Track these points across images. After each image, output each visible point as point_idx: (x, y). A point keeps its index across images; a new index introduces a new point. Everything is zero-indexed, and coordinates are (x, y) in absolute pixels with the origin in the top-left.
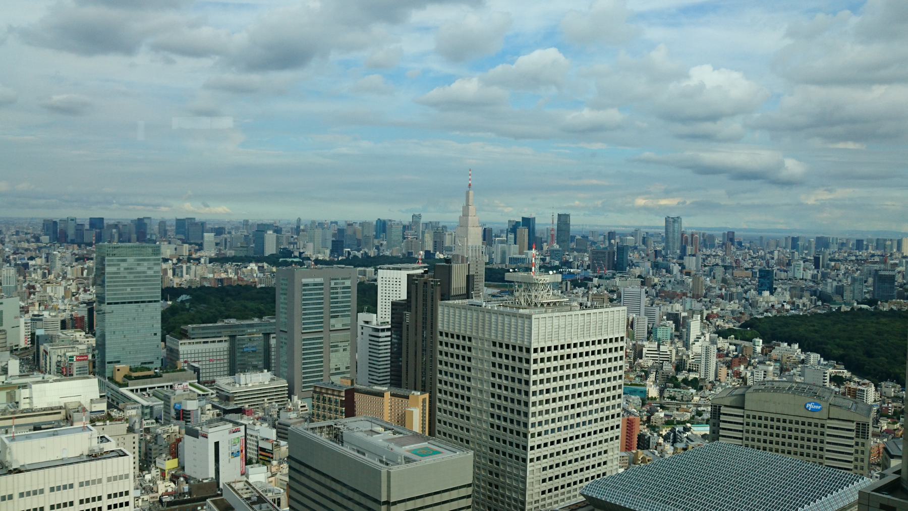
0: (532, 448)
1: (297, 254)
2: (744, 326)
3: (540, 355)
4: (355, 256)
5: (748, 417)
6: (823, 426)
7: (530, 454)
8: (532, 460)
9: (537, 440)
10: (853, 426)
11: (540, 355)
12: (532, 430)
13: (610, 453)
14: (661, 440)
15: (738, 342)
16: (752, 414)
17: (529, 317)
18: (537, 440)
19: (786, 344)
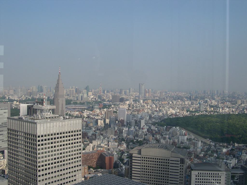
0: (39, 176)
1: (7, 98)
2: (161, 121)
3: (41, 138)
4: (29, 99)
5: (142, 158)
6: (169, 160)
7: (39, 179)
8: (40, 181)
9: (41, 173)
10: (179, 159)
11: (41, 138)
12: (39, 169)
13: (77, 176)
14: (122, 165)
15: (158, 127)
16: (144, 156)
17: (36, 123)
18: (41, 173)
19: (174, 127)
